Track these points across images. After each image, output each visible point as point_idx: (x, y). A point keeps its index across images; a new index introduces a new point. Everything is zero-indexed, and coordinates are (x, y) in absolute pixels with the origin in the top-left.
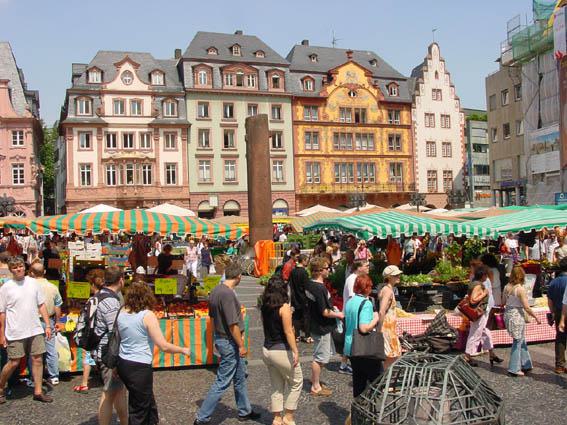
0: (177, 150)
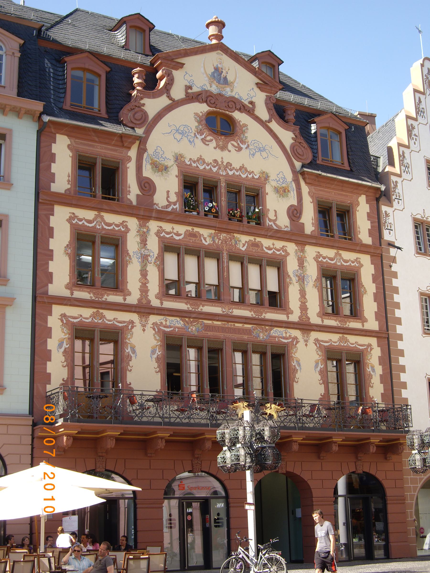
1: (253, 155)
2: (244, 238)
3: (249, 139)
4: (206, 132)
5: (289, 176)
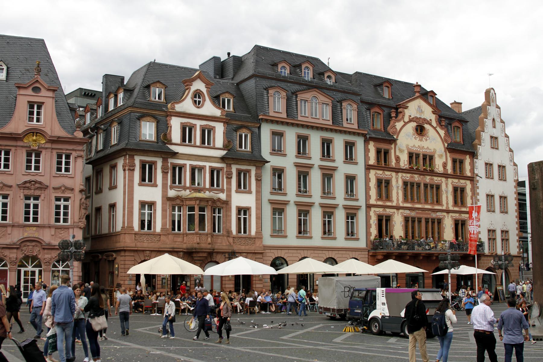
0: (250, 192)
1: (431, 142)
2: (428, 177)
3: (430, 136)
4: (416, 134)
5: (443, 149)
